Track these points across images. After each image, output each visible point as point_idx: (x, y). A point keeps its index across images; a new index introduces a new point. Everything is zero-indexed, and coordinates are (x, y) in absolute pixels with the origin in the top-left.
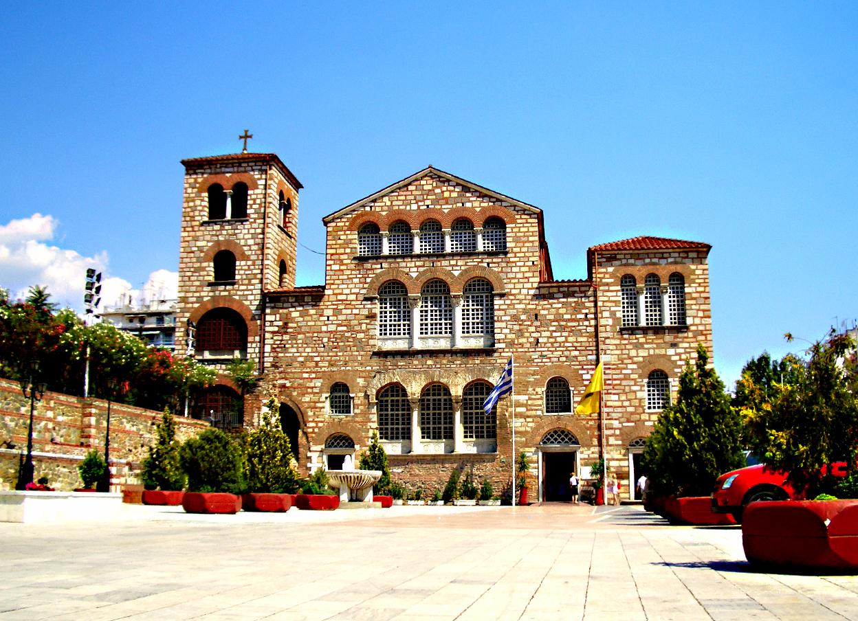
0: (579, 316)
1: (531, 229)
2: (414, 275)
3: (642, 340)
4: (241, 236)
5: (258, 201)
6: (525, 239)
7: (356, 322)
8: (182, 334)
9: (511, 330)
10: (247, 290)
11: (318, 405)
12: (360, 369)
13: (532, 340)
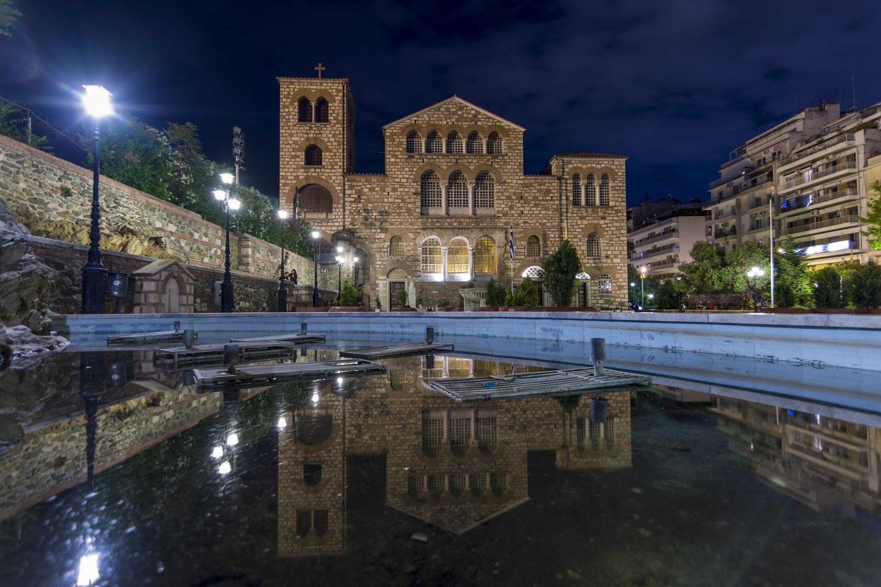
0: (548, 198)
1: (519, 142)
2: (445, 168)
3: (585, 214)
4: (324, 135)
5: (336, 111)
6: (515, 148)
7: (407, 197)
8: (284, 201)
9: (506, 205)
10: (331, 172)
11: (382, 250)
12: (410, 227)
13: (519, 212)
